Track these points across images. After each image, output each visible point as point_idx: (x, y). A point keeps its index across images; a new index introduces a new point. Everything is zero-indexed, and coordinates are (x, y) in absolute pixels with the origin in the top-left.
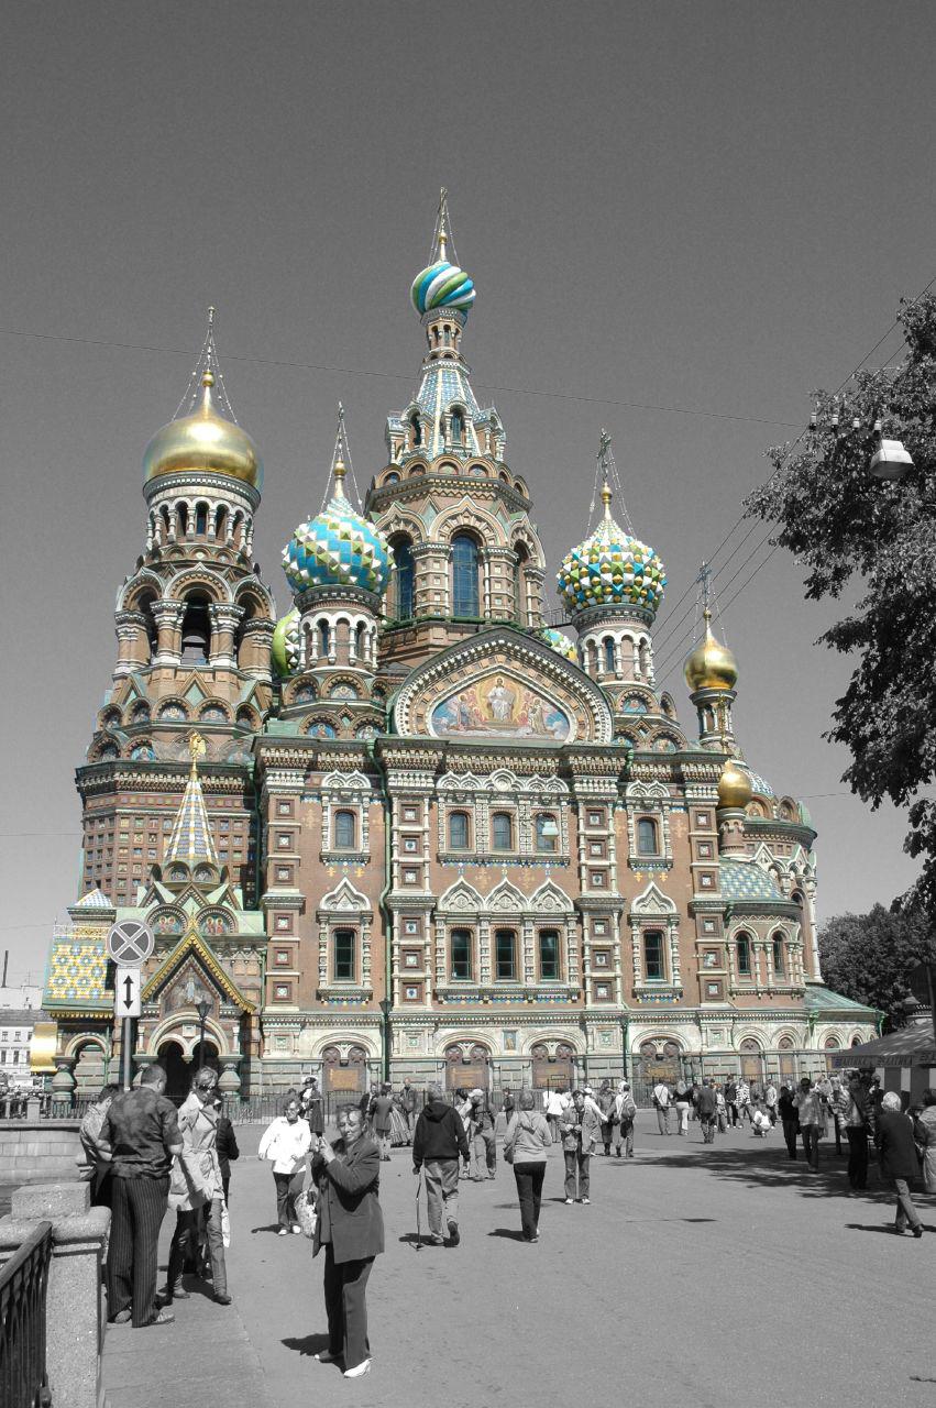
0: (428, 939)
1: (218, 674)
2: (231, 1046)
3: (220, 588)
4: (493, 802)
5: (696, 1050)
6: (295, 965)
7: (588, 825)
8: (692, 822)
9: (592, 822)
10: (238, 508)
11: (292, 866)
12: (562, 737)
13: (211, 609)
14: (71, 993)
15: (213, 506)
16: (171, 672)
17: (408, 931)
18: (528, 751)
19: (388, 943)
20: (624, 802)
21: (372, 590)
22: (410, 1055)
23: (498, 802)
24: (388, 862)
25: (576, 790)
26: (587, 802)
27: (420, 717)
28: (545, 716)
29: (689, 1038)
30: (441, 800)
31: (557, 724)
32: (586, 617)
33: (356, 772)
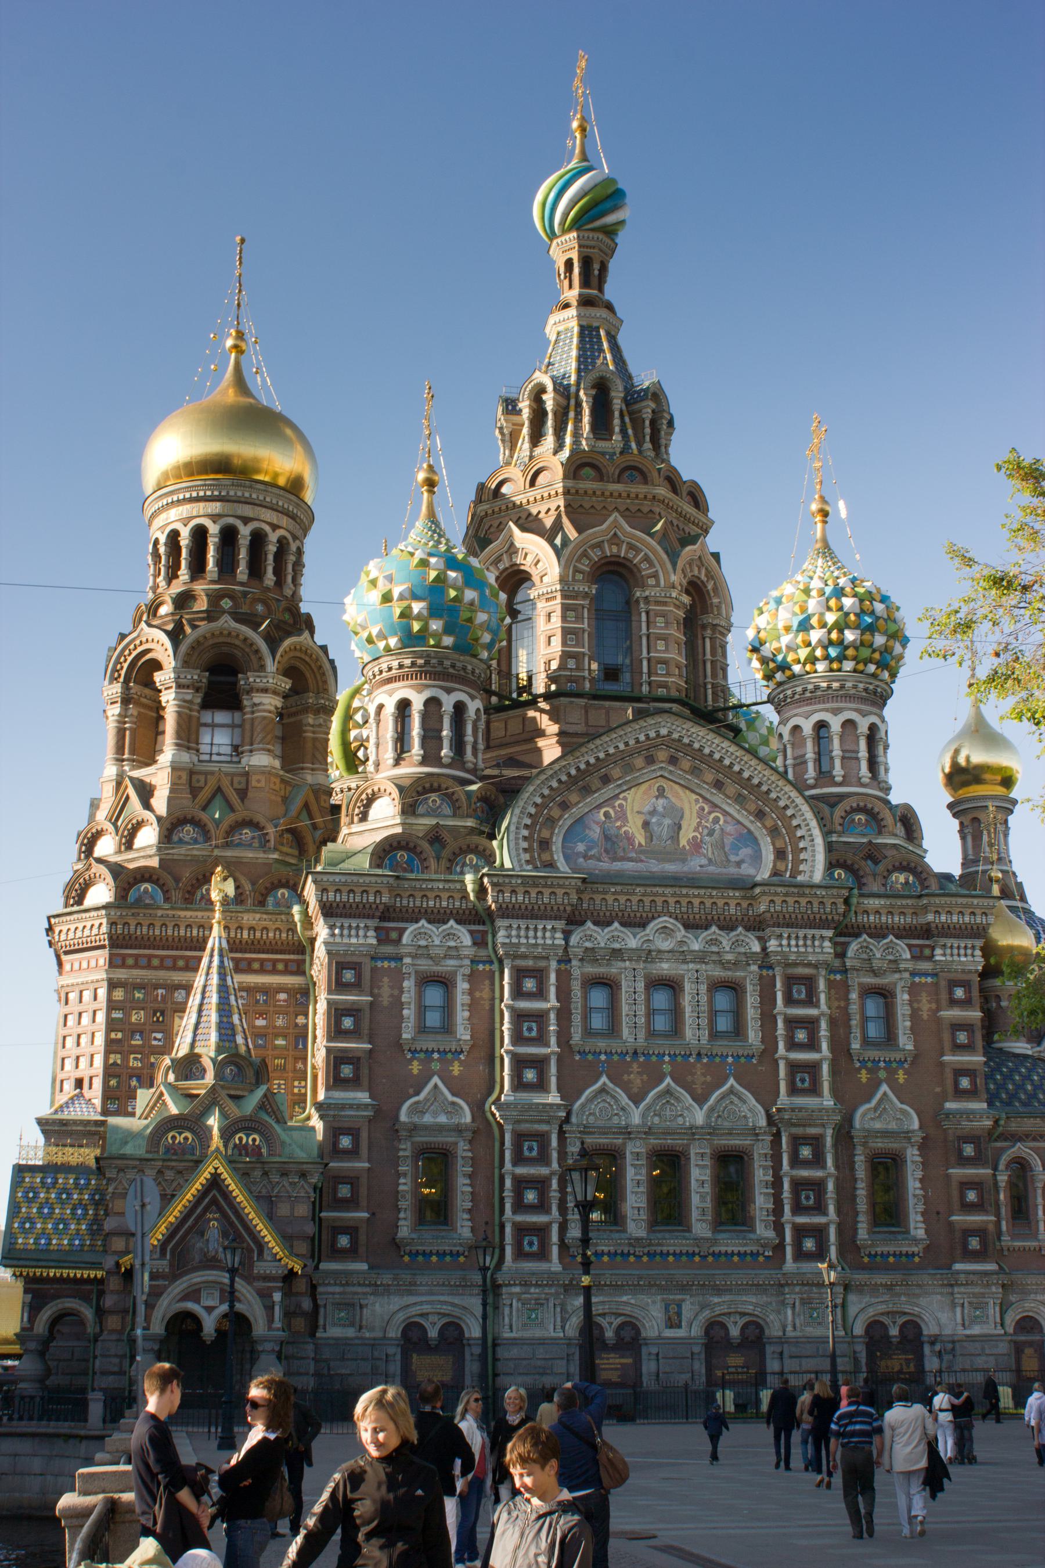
2: (271, 1320)
4: (648, 965)
5: (947, 1331)
6: (364, 1202)
7: (789, 1001)
8: (944, 996)
9: (796, 996)
10: (281, 532)
11: (359, 1059)
12: (751, 871)
14: (43, 1241)
15: (245, 531)
16: (185, 776)
17: (526, 1153)
18: (702, 892)
19: (497, 1171)
20: (844, 964)
21: (475, 656)
22: (527, 1334)
26: (788, 965)
27: (545, 845)
29: (939, 1315)
30: (574, 963)
31: (745, 852)
32: (789, 692)
33: (452, 922)
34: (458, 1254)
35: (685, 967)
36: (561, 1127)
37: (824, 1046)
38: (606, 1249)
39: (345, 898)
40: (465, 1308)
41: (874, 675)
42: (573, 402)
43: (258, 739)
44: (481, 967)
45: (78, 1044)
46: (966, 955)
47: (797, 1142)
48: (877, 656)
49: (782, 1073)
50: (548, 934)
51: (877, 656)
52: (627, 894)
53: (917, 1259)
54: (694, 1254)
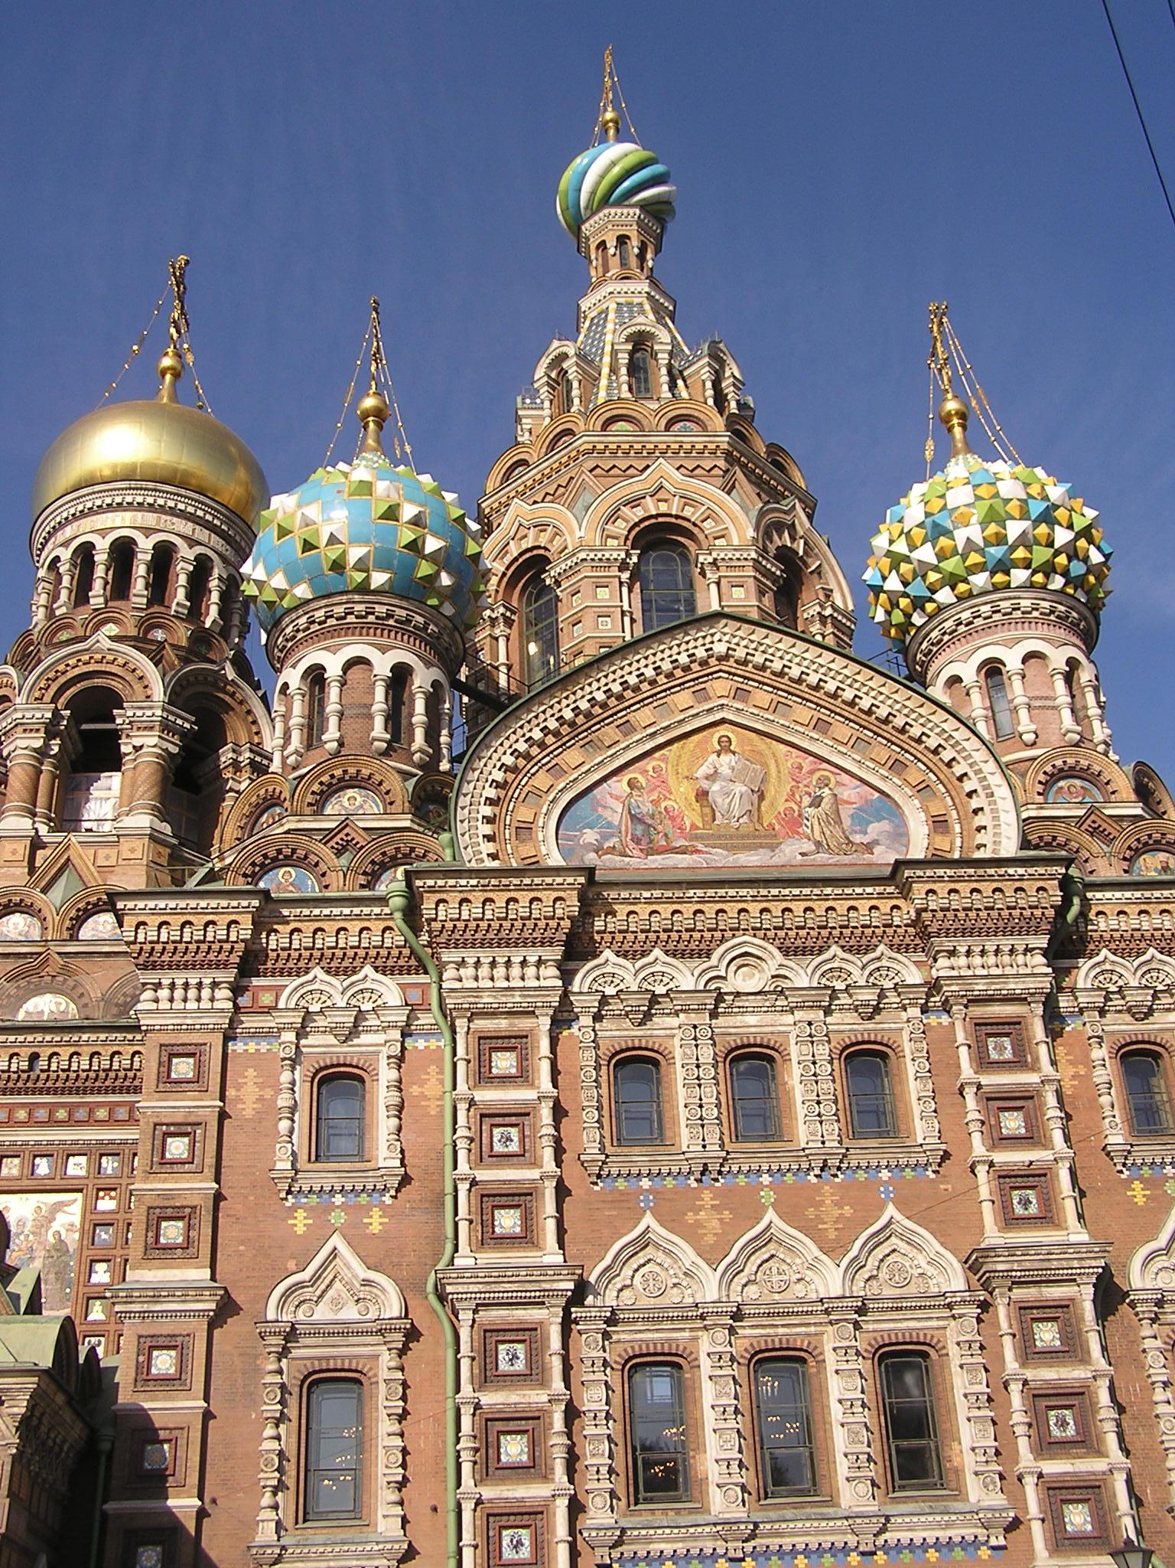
0: (558, 1385)
1: (126, 845)
3: (141, 678)
7: (983, 1063)
9: (994, 1056)
10: (199, 550)
13: (119, 721)
16: (22, 849)
17: (504, 1366)
18: (806, 891)
23: (738, 1020)
24: (449, 1188)
25: (941, 973)
27: (524, 830)
28: (846, 813)
30: (586, 1020)
31: (876, 829)
35: (789, 1019)
38: (668, 1548)
41: (1062, 591)
42: (605, 371)
43: (137, 796)
44: (421, 1044)
47: (1029, 1314)
48: (1062, 559)
49: (984, 1192)
50: (531, 971)
51: (1062, 559)
52: (670, 901)
54: (846, 1549)
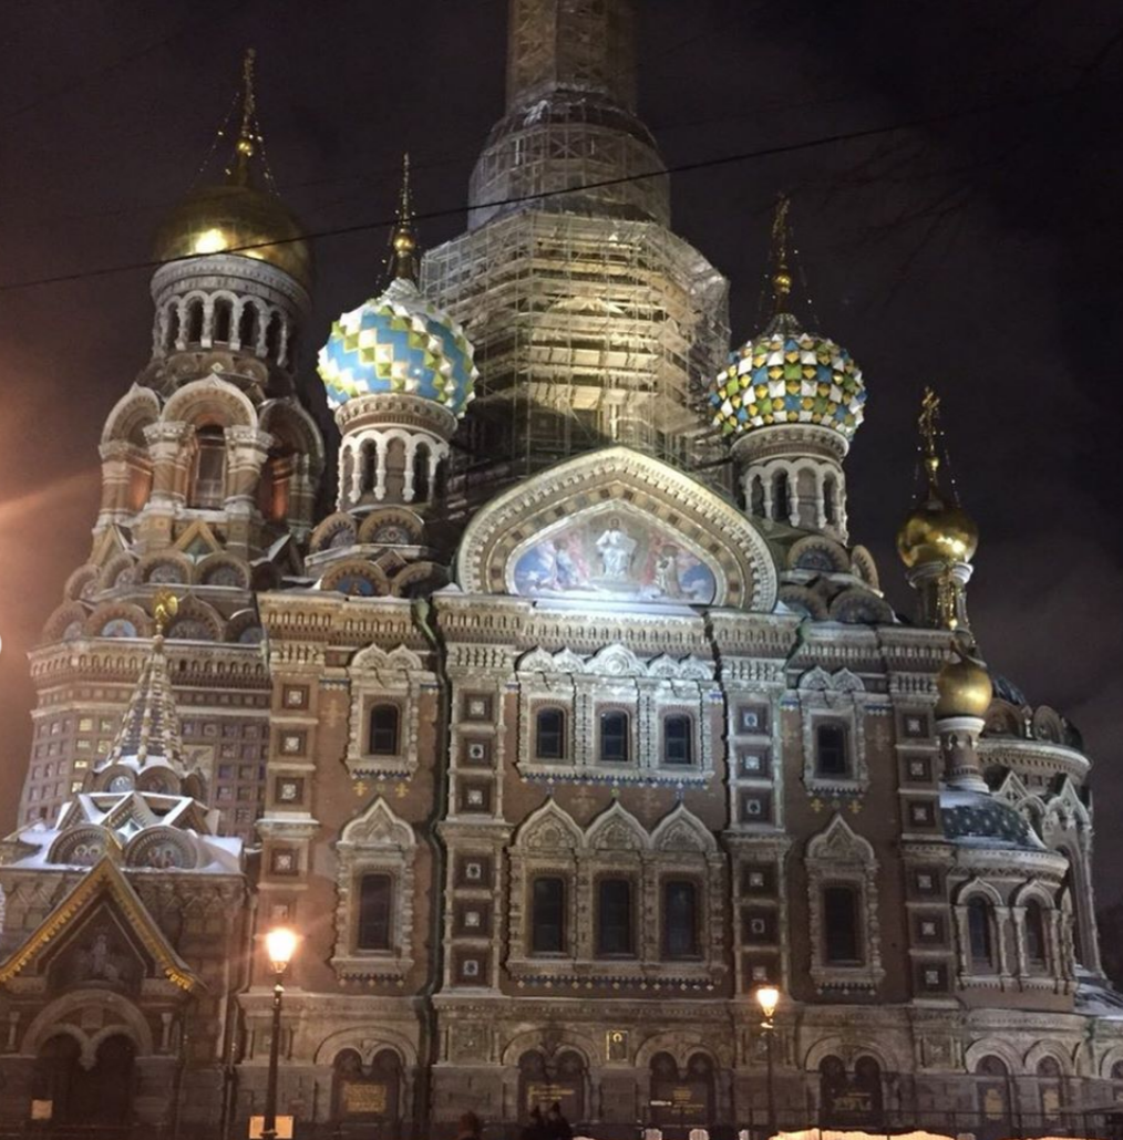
0: (498, 888)
7: (741, 730)
11: (302, 779)
27: (497, 573)
29: (896, 1051)
31: (698, 584)
33: (403, 647)
34: (397, 978)
36: (505, 850)
37: (777, 774)
39: (293, 621)
40: (399, 1034)
45: (46, 775)
46: (921, 689)
53: (872, 993)
54: (640, 981)
